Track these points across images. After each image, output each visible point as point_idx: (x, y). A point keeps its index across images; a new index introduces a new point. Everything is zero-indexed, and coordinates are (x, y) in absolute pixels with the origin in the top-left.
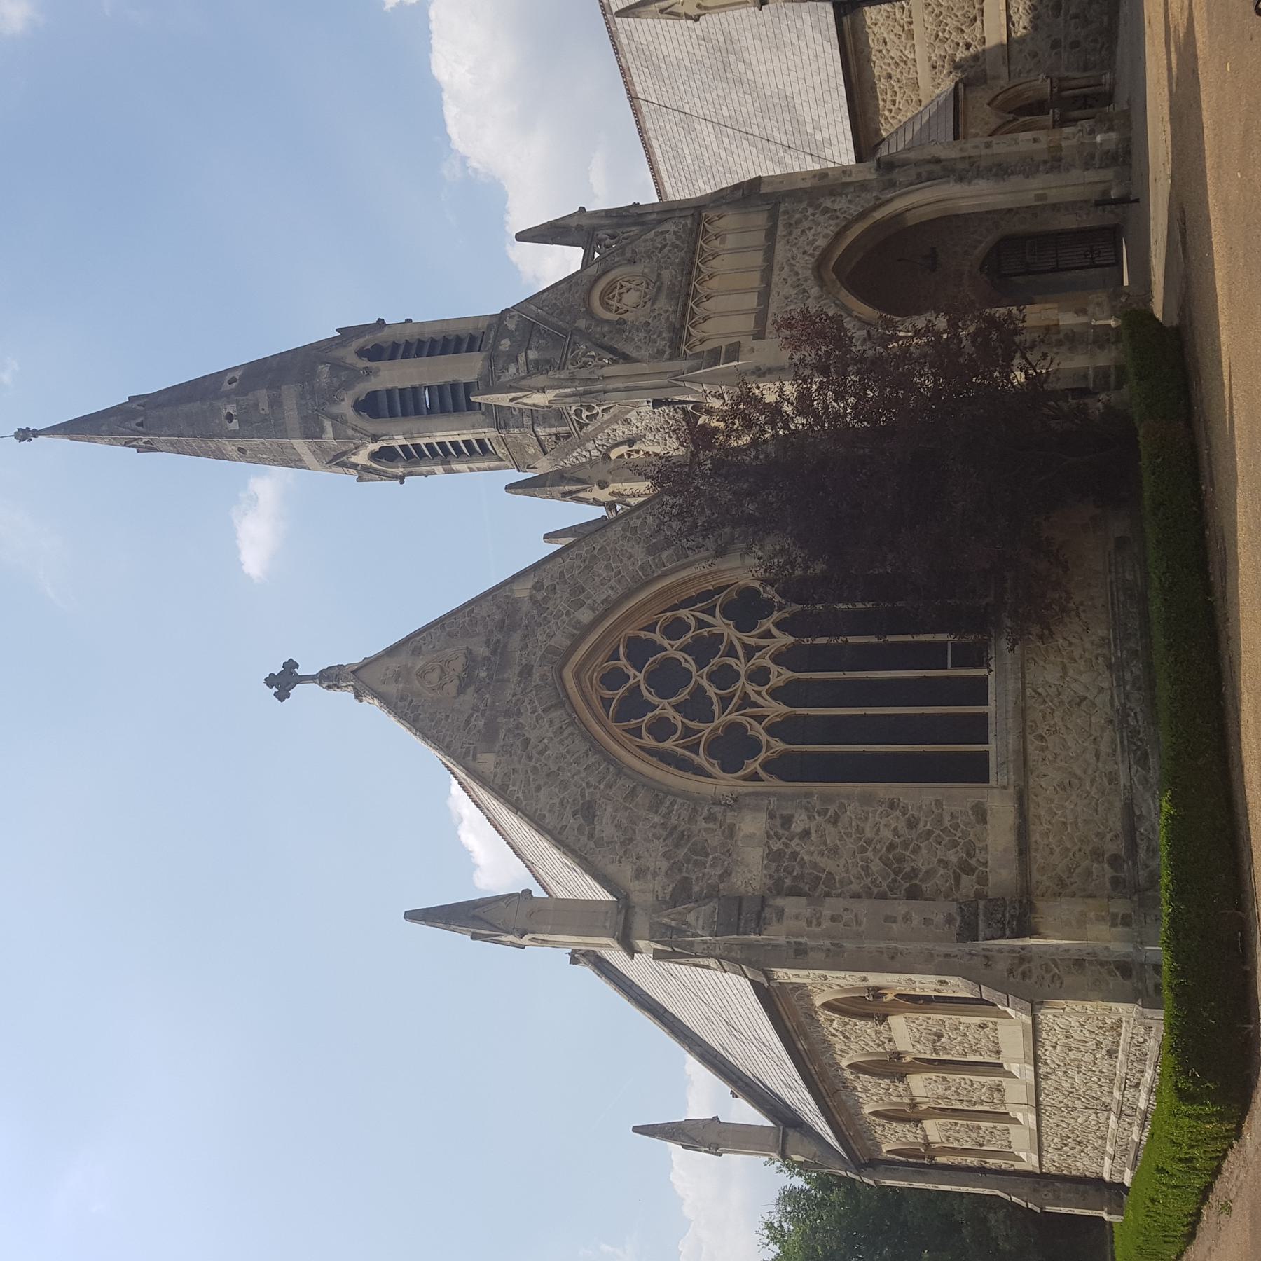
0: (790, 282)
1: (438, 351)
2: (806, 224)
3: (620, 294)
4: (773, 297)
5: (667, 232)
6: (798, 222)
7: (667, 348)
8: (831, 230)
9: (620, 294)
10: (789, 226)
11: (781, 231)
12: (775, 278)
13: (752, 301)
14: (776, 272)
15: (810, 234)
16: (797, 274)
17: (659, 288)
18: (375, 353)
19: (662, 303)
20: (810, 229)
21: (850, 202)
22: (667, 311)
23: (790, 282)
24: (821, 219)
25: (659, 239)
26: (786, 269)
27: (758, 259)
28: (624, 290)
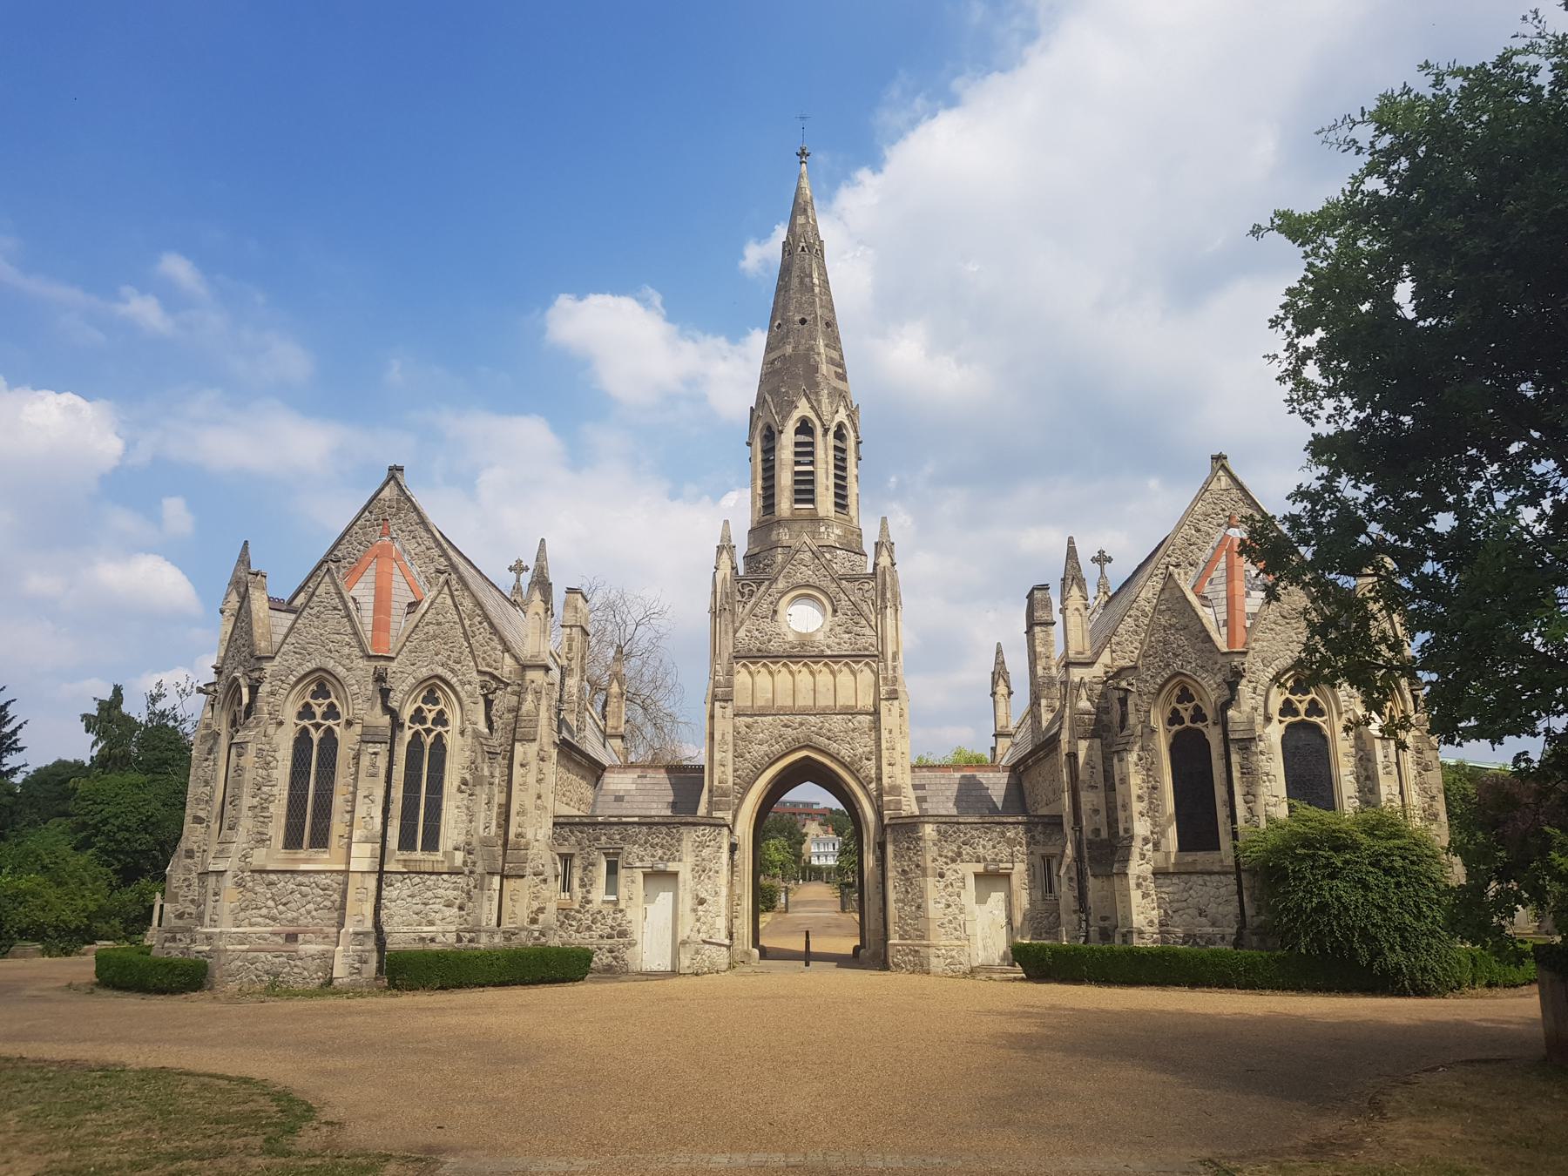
1: (839, 472)
18: (840, 435)
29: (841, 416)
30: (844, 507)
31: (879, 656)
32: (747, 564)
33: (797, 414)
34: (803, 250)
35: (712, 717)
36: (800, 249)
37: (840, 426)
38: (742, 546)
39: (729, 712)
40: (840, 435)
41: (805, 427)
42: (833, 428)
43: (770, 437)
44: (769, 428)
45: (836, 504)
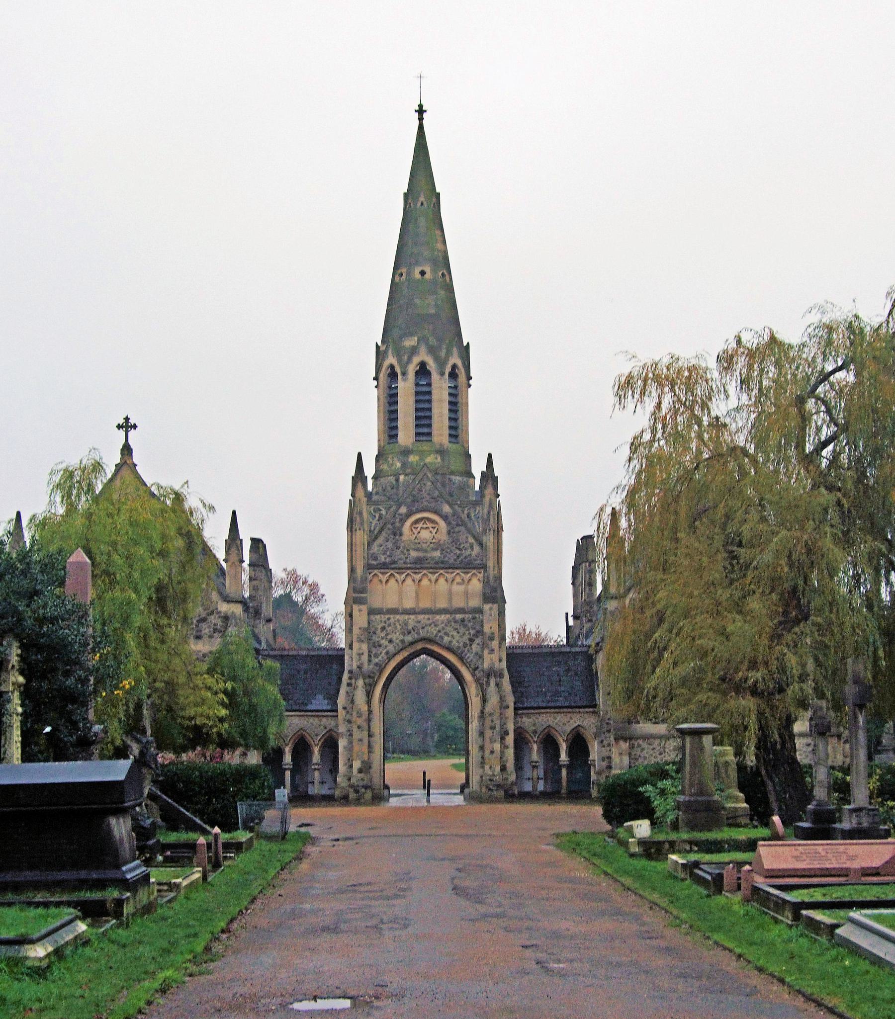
0: (417, 625)
2: (462, 630)
3: (427, 528)
4: (406, 617)
5: (472, 549)
6: (465, 626)
7: (378, 562)
8: (455, 643)
9: (427, 528)
10: (463, 620)
11: (459, 617)
12: (420, 617)
13: (409, 604)
14: (427, 616)
15: (455, 634)
16: (423, 628)
17: (426, 551)
19: (414, 554)
20: (458, 632)
21: (477, 654)
22: (407, 558)
23: (417, 625)
24: (466, 639)
25: (466, 546)
26: (429, 622)
27: (442, 604)
28: (431, 529)
29: (455, 359)
30: (456, 436)
31: (483, 567)
32: (374, 485)
33: (416, 360)
34: (422, 204)
35: (351, 615)
36: (419, 204)
37: (454, 367)
38: (370, 470)
39: (365, 612)
40: (453, 375)
41: (423, 371)
42: (448, 370)
43: (393, 375)
44: (392, 367)
45: (450, 435)
